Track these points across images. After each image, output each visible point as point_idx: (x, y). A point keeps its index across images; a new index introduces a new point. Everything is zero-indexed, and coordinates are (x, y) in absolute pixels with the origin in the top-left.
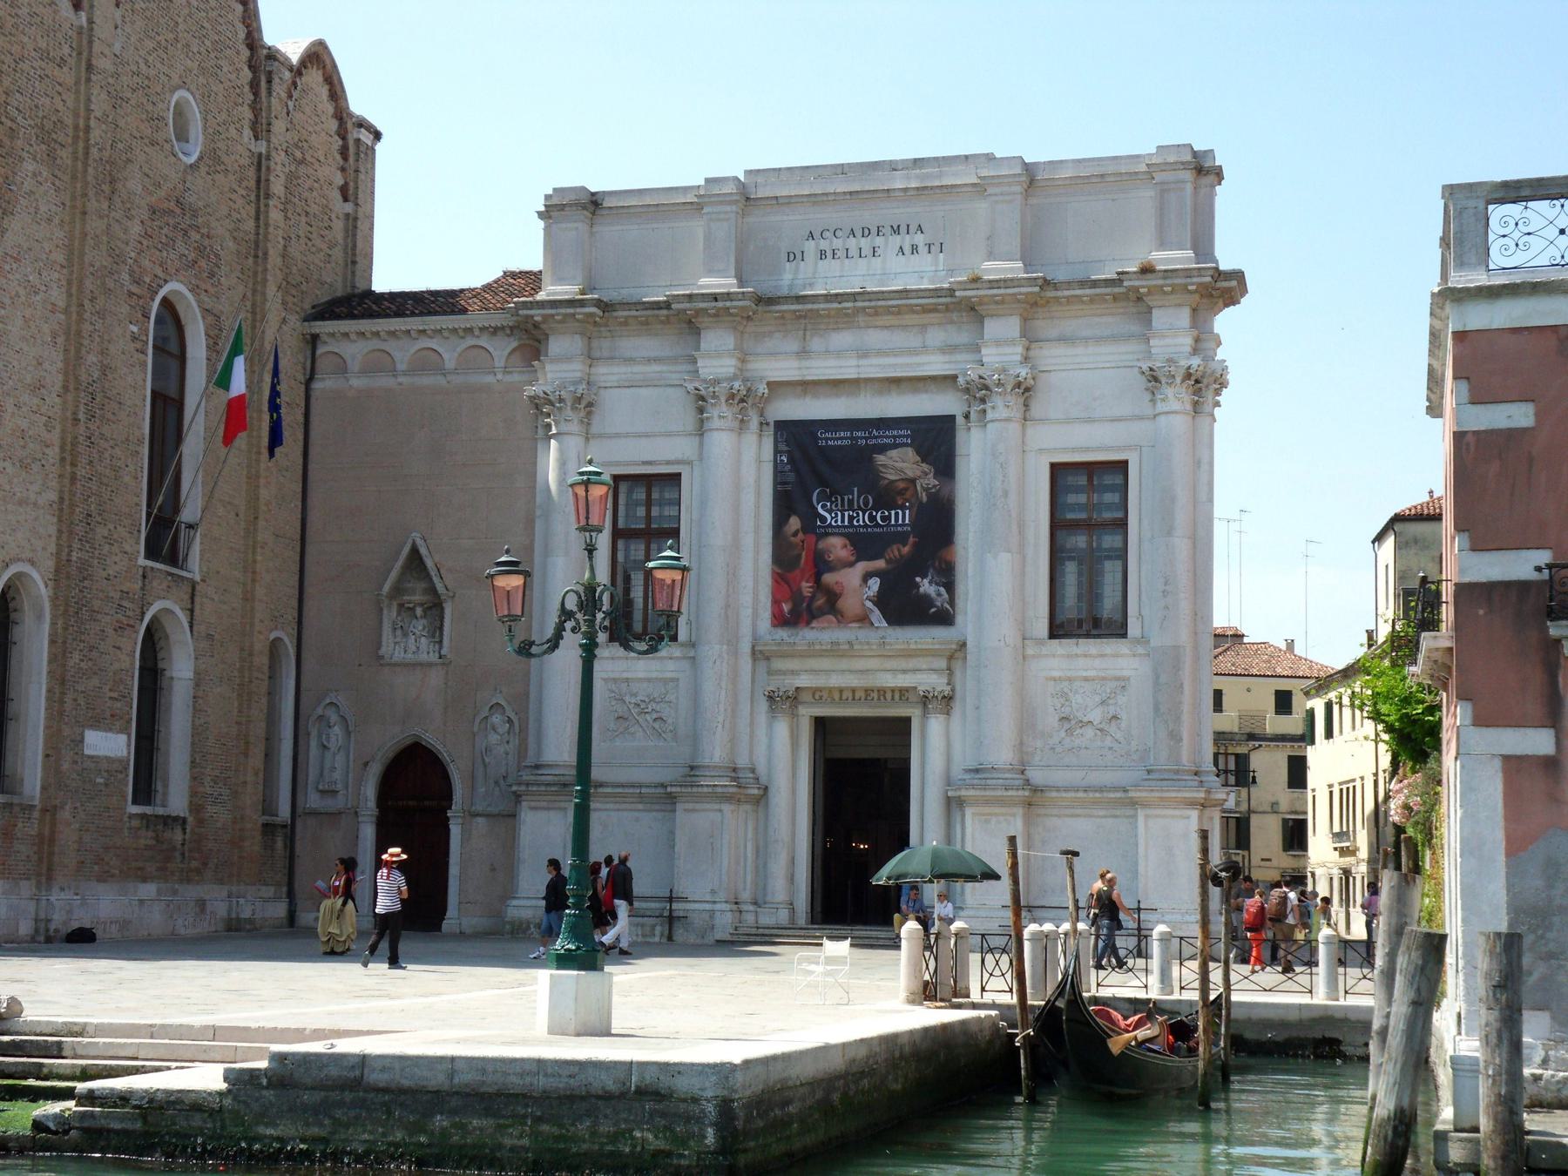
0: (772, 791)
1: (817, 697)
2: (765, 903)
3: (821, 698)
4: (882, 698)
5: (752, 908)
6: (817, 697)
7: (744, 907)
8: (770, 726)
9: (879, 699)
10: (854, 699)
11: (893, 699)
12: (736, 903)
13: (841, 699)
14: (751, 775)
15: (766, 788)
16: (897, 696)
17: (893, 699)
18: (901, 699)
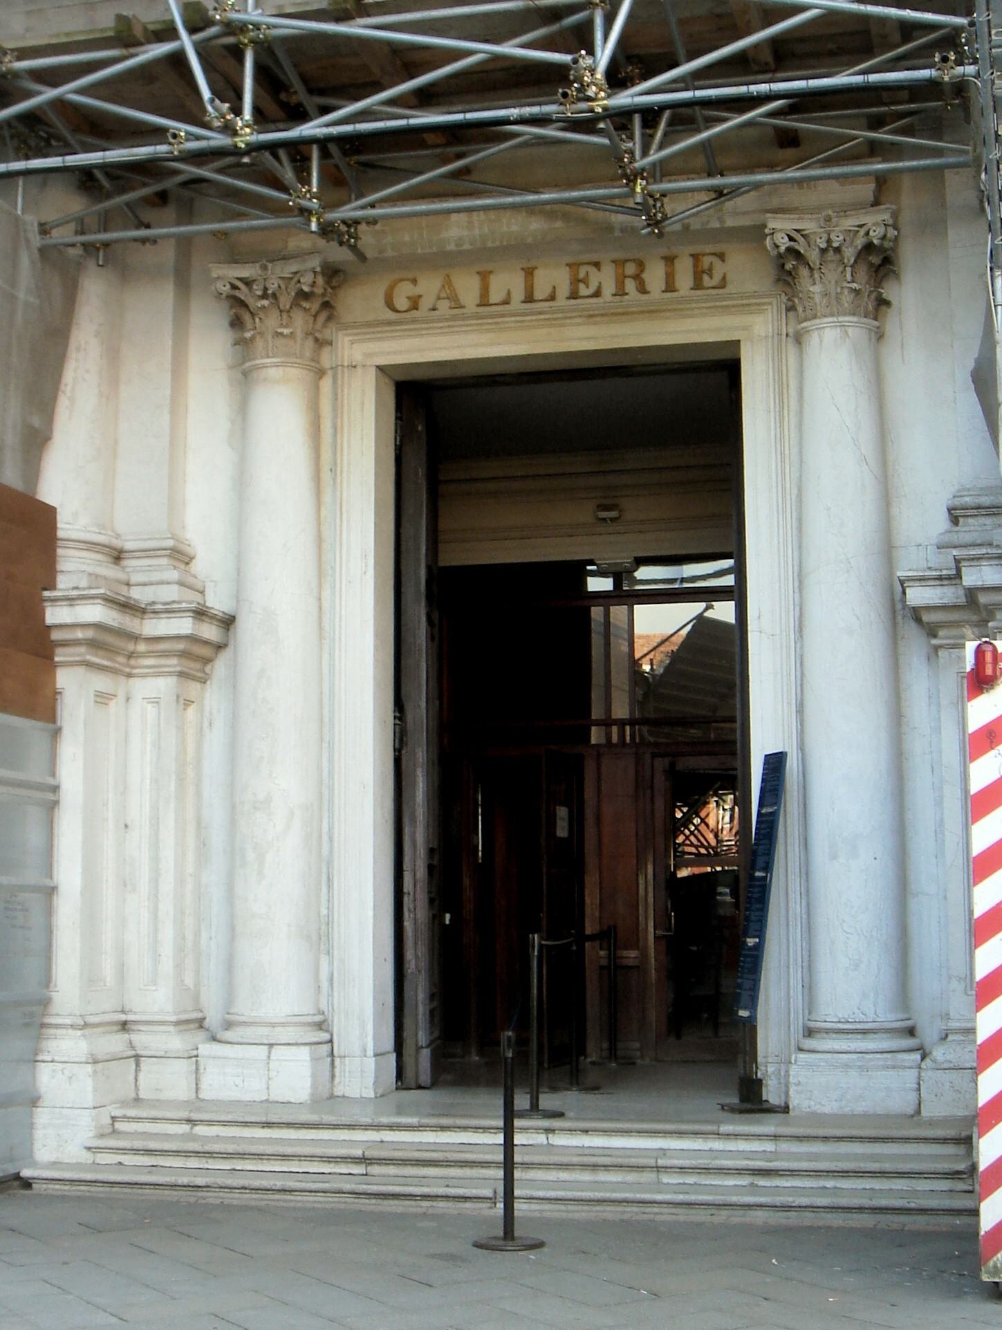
0: (247, 627)
1: (401, 303)
2: (228, 1025)
3: (415, 304)
4: (630, 285)
5: (175, 1042)
6: (401, 303)
7: (145, 1040)
8: (242, 409)
9: (620, 292)
10: (529, 299)
11: (670, 287)
12: (124, 1026)
13: (484, 302)
14: (174, 575)
15: (228, 622)
16: (684, 280)
17: (670, 287)
18: (698, 285)
